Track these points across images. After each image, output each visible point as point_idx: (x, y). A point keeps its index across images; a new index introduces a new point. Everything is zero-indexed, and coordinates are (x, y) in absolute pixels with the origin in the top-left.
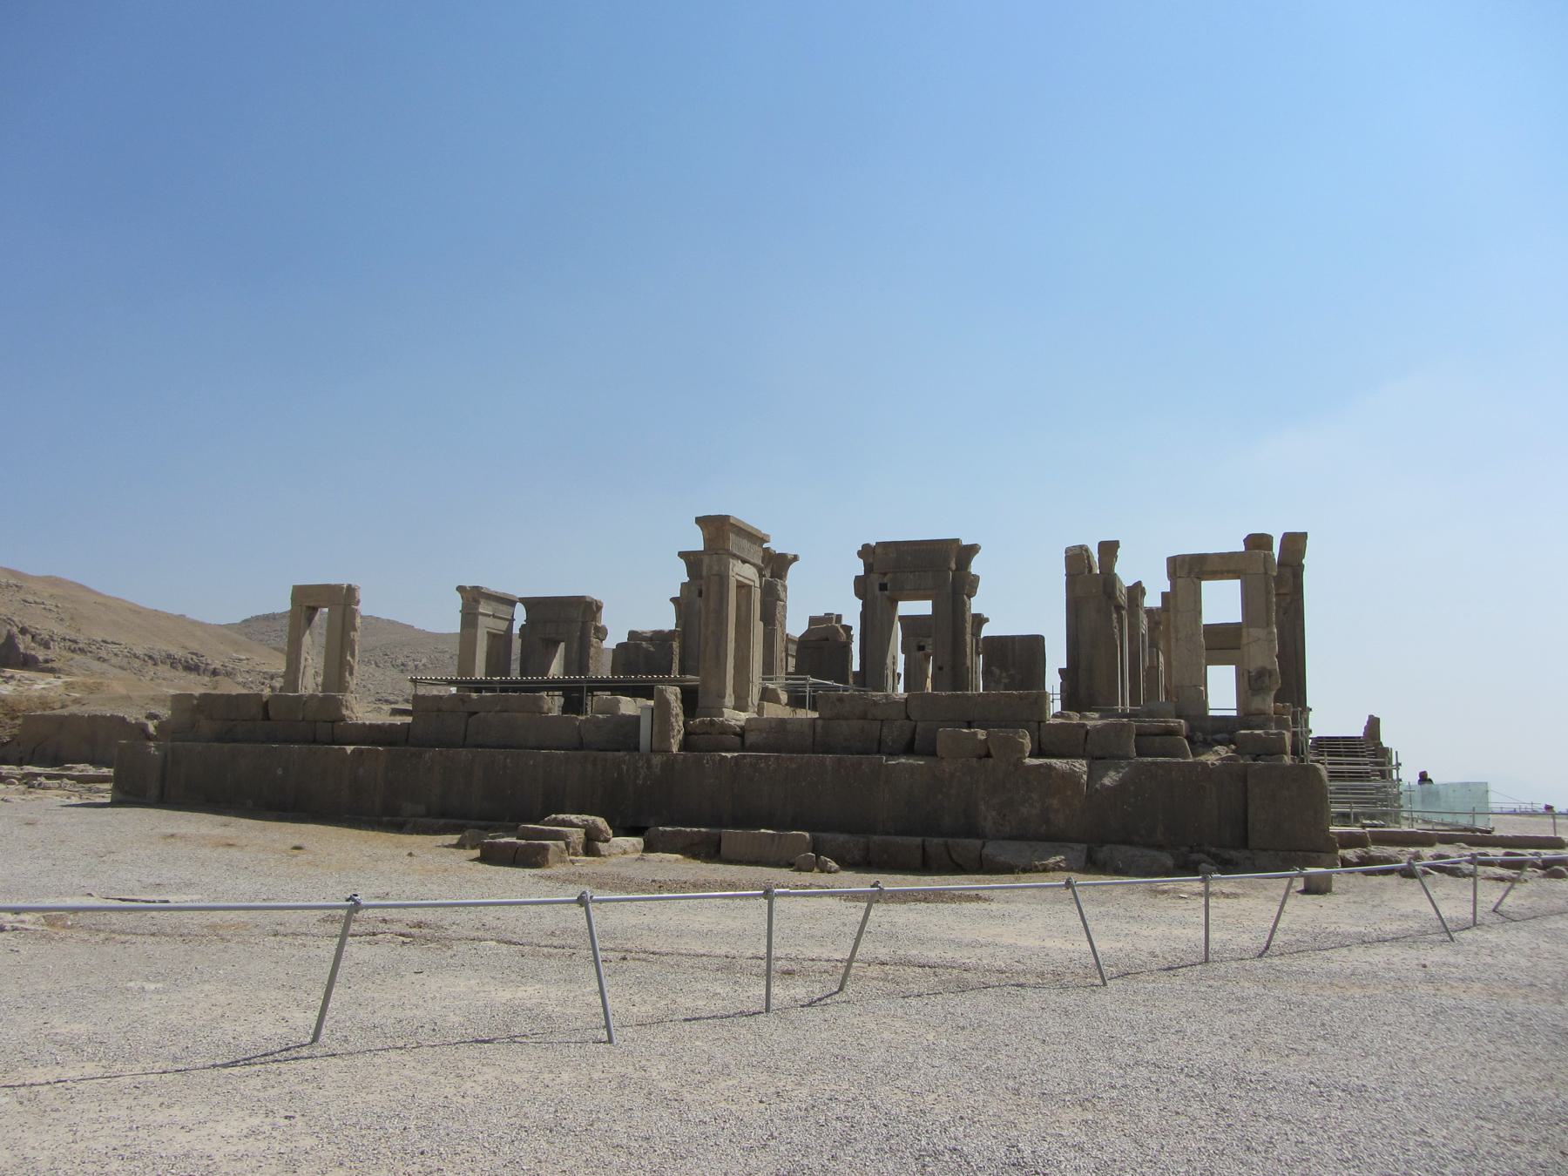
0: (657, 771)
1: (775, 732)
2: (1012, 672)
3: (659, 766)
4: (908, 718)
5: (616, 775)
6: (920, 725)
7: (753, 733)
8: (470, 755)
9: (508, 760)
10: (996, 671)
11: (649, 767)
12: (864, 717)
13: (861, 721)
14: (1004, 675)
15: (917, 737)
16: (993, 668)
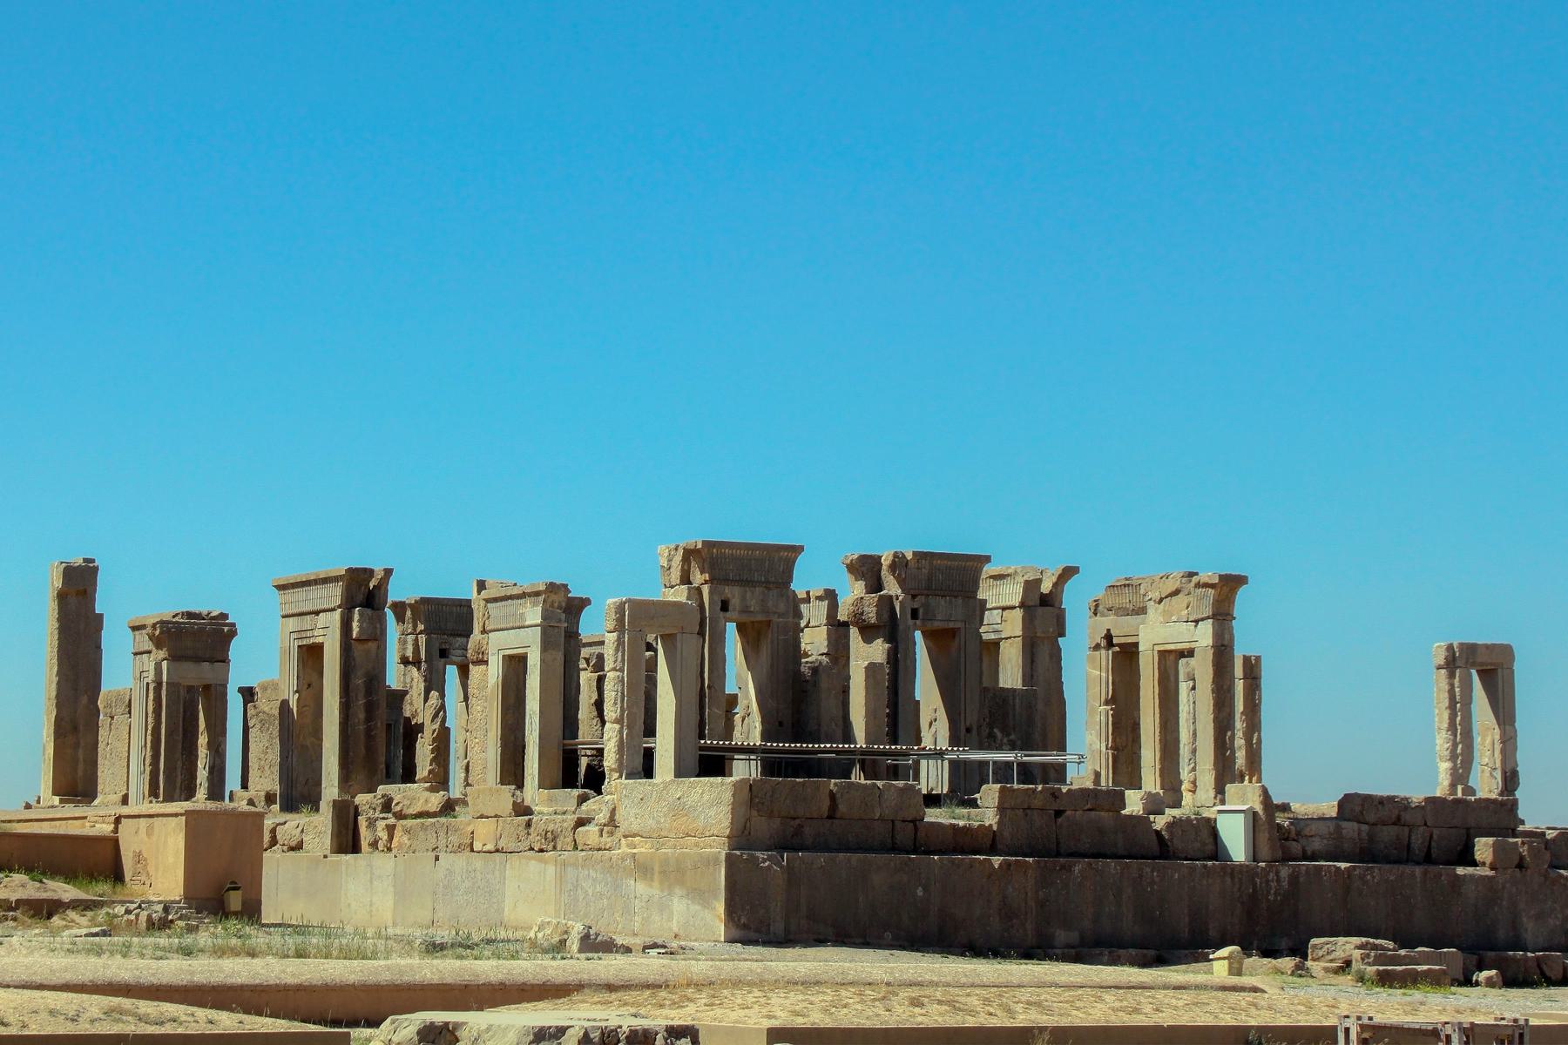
0: (1285, 884)
1: (1334, 839)
2: (1012, 737)
3: (1287, 879)
4: (1425, 824)
5: (1251, 890)
6: (1436, 832)
7: (1314, 839)
8: (1118, 868)
9: (1155, 874)
10: (999, 735)
11: (1278, 881)
12: (1398, 821)
13: (1396, 827)
14: (1005, 740)
15: (1433, 844)
16: (995, 730)
